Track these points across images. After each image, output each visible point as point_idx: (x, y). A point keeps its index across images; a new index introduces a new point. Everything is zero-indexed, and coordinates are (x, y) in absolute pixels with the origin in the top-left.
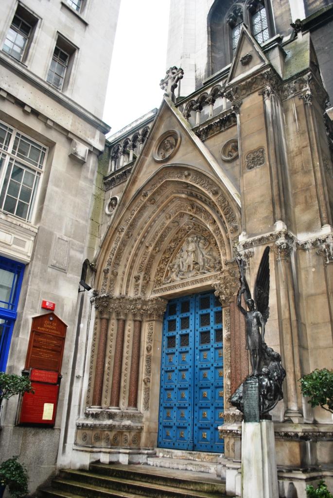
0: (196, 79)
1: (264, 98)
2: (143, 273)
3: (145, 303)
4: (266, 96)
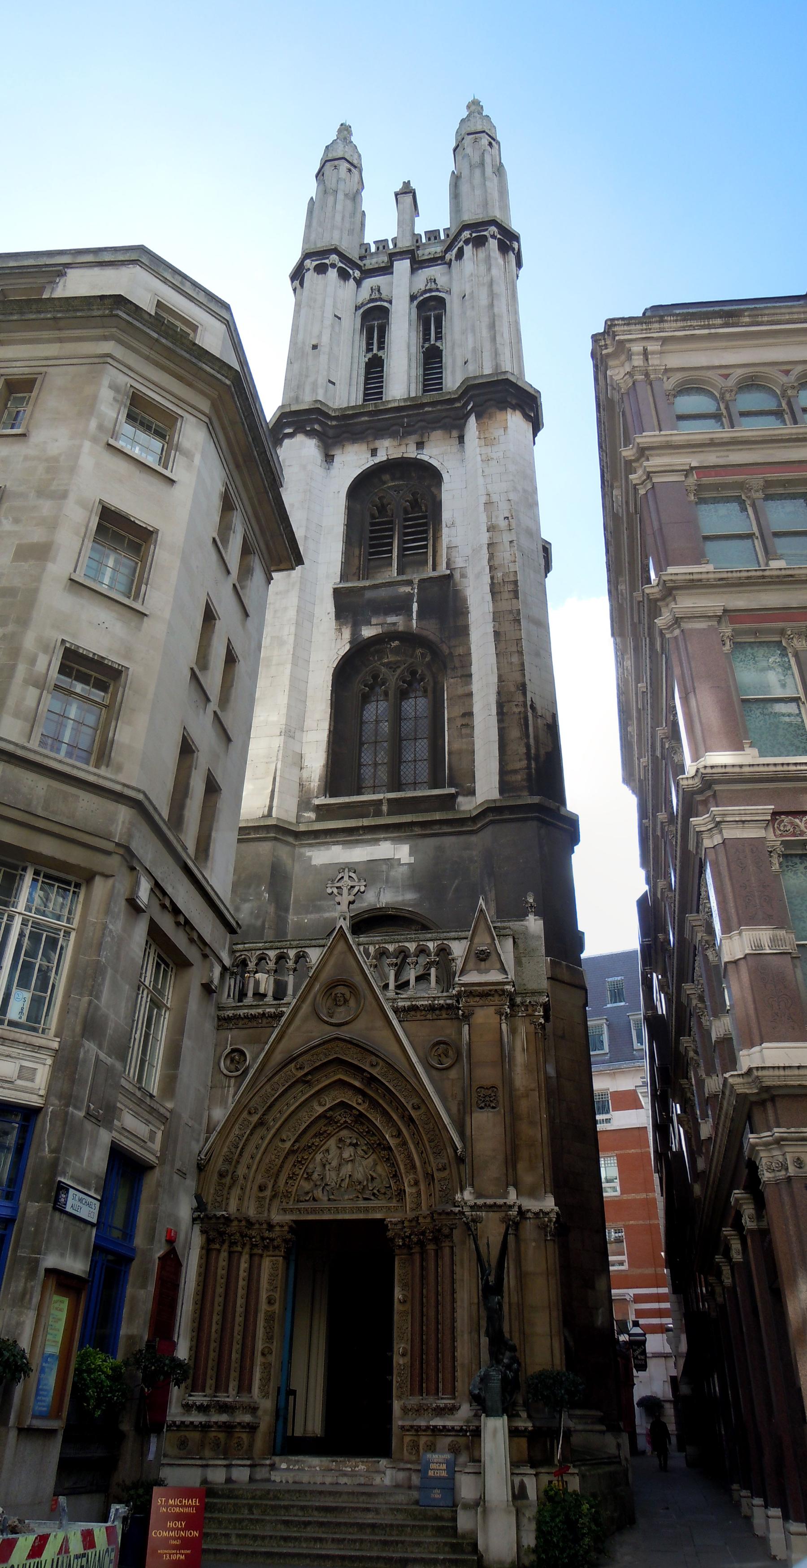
0: (301, 785)
1: (501, 1020)
2: (272, 1181)
3: (271, 1227)
4: (503, 1018)
